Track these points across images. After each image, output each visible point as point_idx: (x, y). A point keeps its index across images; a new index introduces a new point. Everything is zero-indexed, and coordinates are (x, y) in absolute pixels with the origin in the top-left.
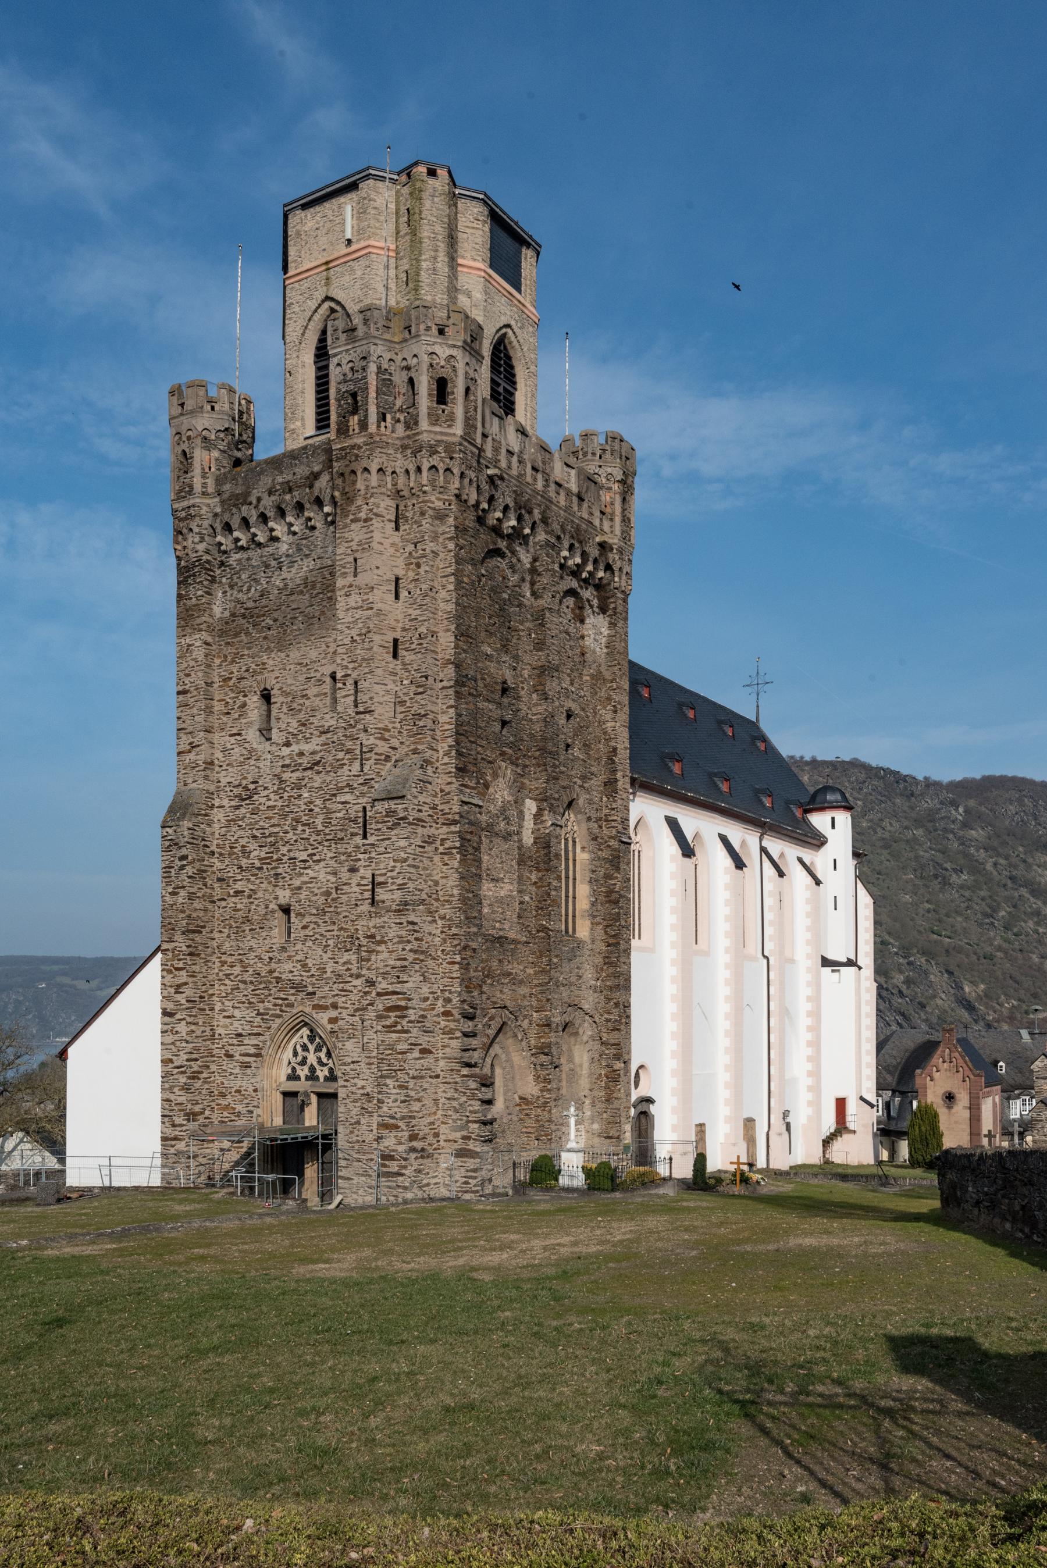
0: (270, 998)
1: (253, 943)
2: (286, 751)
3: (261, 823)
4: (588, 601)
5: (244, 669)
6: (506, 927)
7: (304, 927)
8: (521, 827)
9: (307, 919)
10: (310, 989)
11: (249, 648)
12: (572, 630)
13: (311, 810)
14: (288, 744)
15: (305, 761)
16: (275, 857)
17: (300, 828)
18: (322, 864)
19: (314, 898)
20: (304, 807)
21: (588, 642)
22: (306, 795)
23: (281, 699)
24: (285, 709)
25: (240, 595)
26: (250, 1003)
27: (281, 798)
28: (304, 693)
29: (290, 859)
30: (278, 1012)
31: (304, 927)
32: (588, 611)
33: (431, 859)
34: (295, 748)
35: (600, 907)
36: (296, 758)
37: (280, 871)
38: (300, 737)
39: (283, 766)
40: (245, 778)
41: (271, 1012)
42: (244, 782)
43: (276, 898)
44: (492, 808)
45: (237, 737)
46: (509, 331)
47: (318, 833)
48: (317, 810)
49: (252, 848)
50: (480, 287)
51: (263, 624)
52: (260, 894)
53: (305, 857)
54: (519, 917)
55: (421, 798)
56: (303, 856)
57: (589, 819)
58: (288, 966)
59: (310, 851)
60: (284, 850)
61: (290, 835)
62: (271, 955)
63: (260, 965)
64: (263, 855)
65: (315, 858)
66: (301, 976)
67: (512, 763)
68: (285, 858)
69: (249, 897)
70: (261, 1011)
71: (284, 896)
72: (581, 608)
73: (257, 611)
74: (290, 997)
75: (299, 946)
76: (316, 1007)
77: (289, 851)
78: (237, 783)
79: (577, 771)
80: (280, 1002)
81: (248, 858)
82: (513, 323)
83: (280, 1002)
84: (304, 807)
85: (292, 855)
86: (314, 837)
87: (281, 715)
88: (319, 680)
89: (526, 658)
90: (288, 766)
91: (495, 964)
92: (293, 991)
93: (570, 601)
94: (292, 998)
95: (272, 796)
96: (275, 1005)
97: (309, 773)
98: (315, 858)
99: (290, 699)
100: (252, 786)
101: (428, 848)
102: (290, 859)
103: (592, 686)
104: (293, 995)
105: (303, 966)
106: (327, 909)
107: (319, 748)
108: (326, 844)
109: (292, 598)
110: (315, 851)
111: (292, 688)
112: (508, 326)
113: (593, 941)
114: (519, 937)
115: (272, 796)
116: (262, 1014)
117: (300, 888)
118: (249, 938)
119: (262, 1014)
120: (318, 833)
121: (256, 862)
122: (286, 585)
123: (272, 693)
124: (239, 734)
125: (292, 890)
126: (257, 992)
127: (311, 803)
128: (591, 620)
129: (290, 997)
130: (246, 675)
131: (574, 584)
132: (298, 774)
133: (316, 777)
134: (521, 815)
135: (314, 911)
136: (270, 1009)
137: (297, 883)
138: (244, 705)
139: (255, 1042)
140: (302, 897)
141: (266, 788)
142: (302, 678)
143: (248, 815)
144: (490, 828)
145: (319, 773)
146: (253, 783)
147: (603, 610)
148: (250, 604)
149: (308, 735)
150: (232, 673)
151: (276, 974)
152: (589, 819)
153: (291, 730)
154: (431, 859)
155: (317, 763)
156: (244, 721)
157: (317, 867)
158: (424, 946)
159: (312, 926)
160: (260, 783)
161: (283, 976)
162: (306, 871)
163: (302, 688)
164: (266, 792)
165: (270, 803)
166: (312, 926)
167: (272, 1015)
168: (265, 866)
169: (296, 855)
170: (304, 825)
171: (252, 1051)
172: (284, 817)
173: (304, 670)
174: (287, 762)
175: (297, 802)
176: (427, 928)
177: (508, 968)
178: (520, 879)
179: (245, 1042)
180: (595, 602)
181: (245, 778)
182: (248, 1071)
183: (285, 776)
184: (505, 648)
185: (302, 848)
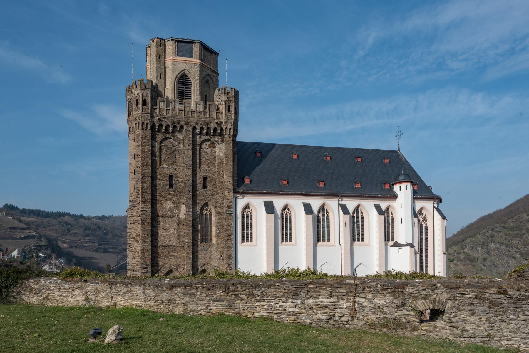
4: (215, 141)
6: (172, 242)
8: (179, 213)
12: (209, 151)
21: (217, 153)
32: (216, 144)
33: (137, 227)
35: (222, 233)
44: (165, 210)
46: (186, 71)
50: (171, 64)
54: (178, 239)
55: (133, 211)
57: (216, 207)
67: (174, 196)
72: (213, 143)
79: (209, 194)
82: (186, 68)
89: (181, 165)
91: (166, 253)
93: (208, 143)
101: (135, 224)
103: (218, 166)
112: (185, 70)
113: (218, 244)
114: (178, 245)
128: (217, 146)
131: (208, 137)
134: (179, 210)
144: (164, 216)
147: (223, 142)
152: (216, 207)
154: (137, 227)
158: (134, 249)
176: (135, 245)
177: (171, 253)
178: (178, 229)
180: (220, 140)
184: (173, 164)
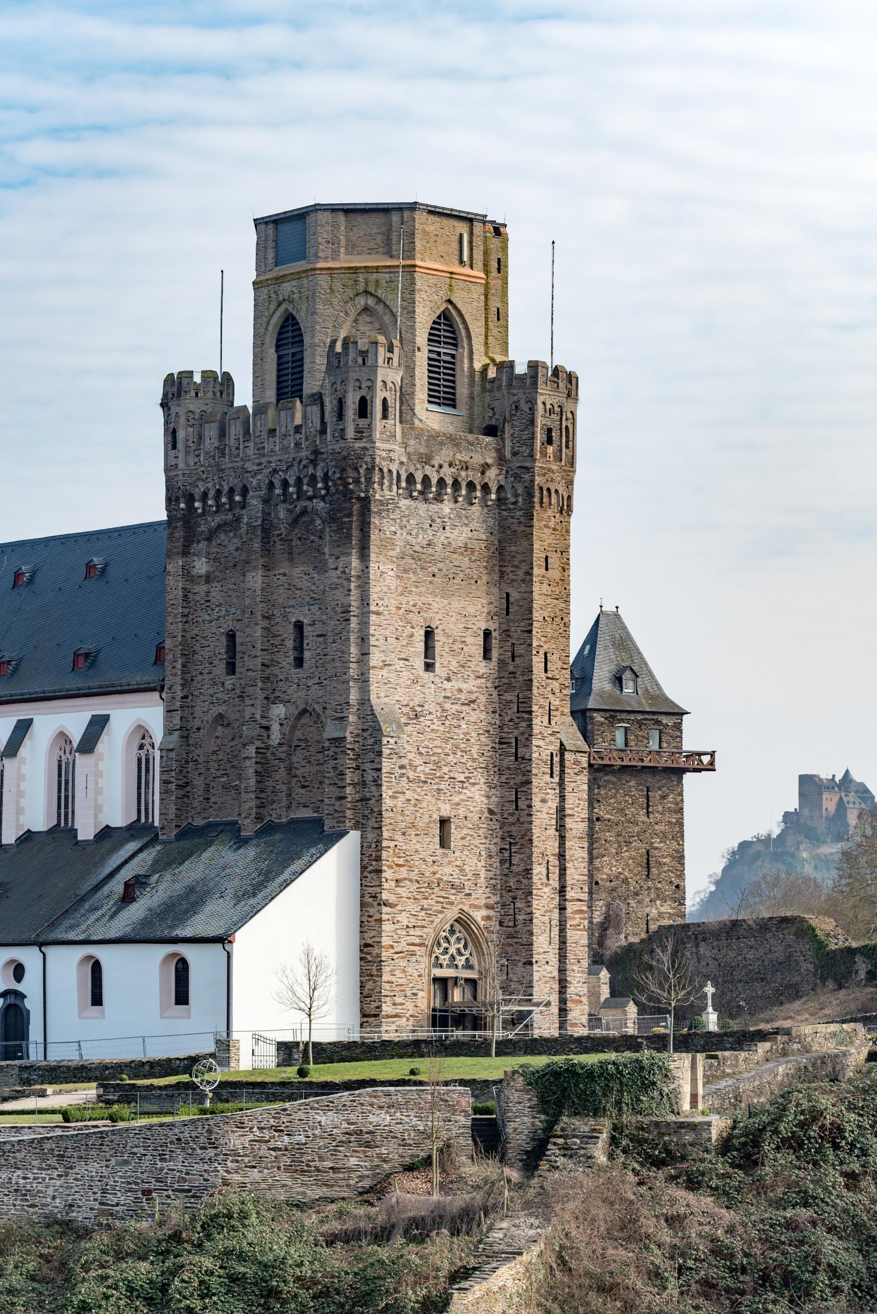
0: (433, 896)
1: (418, 846)
2: (447, 685)
3: (426, 743)
5: (412, 603)
7: (463, 838)
9: (466, 831)
10: (467, 891)
11: (417, 587)
13: (468, 740)
14: (448, 680)
15: (463, 697)
16: (438, 774)
17: (459, 753)
18: (477, 787)
19: (471, 815)
20: (462, 736)
22: (464, 726)
23: (443, 639)
24: (447, 649)
25: (409, 537)
26: (415, 899)
27: (443, 724)
28: (463, 639)
29: (450, 778)
30: (440, 908)
31: (463, 838)
34: (455, 684)
36: (456, 693)
37: (442, 787)
38: (459, 676)
39: (445, 697)
40: (412, 700)
41: (434, 908)
42: (411, 704)
43: (439, 809)
45: (406, 662)
47: (474, 760)
48: (472, 740)
49: (418, 763)
51: (429, 570)
52: (424, 805)
53: (463, 779)
56: (461, 777)
58: (448, 870)
59: (467, 775)
60: (446, 769)
61: (451, 758)
62: (434, 858)
63: (424, 867)
64: (427, 770)
65: (471, 781)
66: (459, 878)
68: (446, 777)
69: (415, 806)
70: (425, 906)
71: (446, 810)
73: (423, 556)
74: (451, 897)
75: (458, 854)
76: (471, 906)
77: (450, 771)
78: (405, 703)
80: (442, 900)
81: (415, 771)
83: (442, 900)
84: (462, 736)
85: (452, 775)
86: (470, 763)
87: (444, 653)
88: (476, 633)
90: (448, 698)
92: (453, 891)
94: (453, 897)
95: (435, 721)
96: (438, 902)
97: (466, 708)
98: (471, 781)
99: (451, 641)
100: (418, 709)
102: (450, 778)
104: (454, 894)
105: (462, 870)
106: (481, 825)
107: (475, 689)
108: (480, 770)
109: (455, 556)
110: (470, 775)
111: (453, 632)
115: (435, 721)
116: (426, 910)
117: (458, 804)
118: (414, 842)
119: (426, 910)
120: (474, 760)
121: (422, 775)
122: (449, 543)
123: (436, 631)
124: (407, 660)
125: (451, 804)
126: (423, 890)
127: (467, 733)
129: (451, 897)
130: (413, 609)
132: (457, 707)
133: (472, 713)
135: (471, 826)
136: (433, 905)
137: (456, 799)
138: (412, 636)
139: (420, 933)
140: (460, 812)
141: (430, 713)
142: (461, 626)
143: (415, 734)
145: (474, 710)
146: (419, 706)
148: (418, 548)
149: (466, 677)
150: (401, 604)
151: (438, 876)
153: (452, 668)
155: (473, 702)
156: (412, 649)
157: (472, 789)
159: (469, 838)
160: (426, 707)
161: (445, 878)
162: (464, 791)
163: (461, 634)
164: (431, 717)
165: (434, 727)
166: (469, 838)
167: (435, 911)
168: (429, 781)
169: (456, 776)
170: (462, 751)
171: (417, 941)
172: (446, 741)
173: (463, 620)
174: (449, 694)
175: (456, 730)
179: (411, 933)
181: (412, 700)
182: (414, 959)
183: (447, 706)
185: (460, 770)
